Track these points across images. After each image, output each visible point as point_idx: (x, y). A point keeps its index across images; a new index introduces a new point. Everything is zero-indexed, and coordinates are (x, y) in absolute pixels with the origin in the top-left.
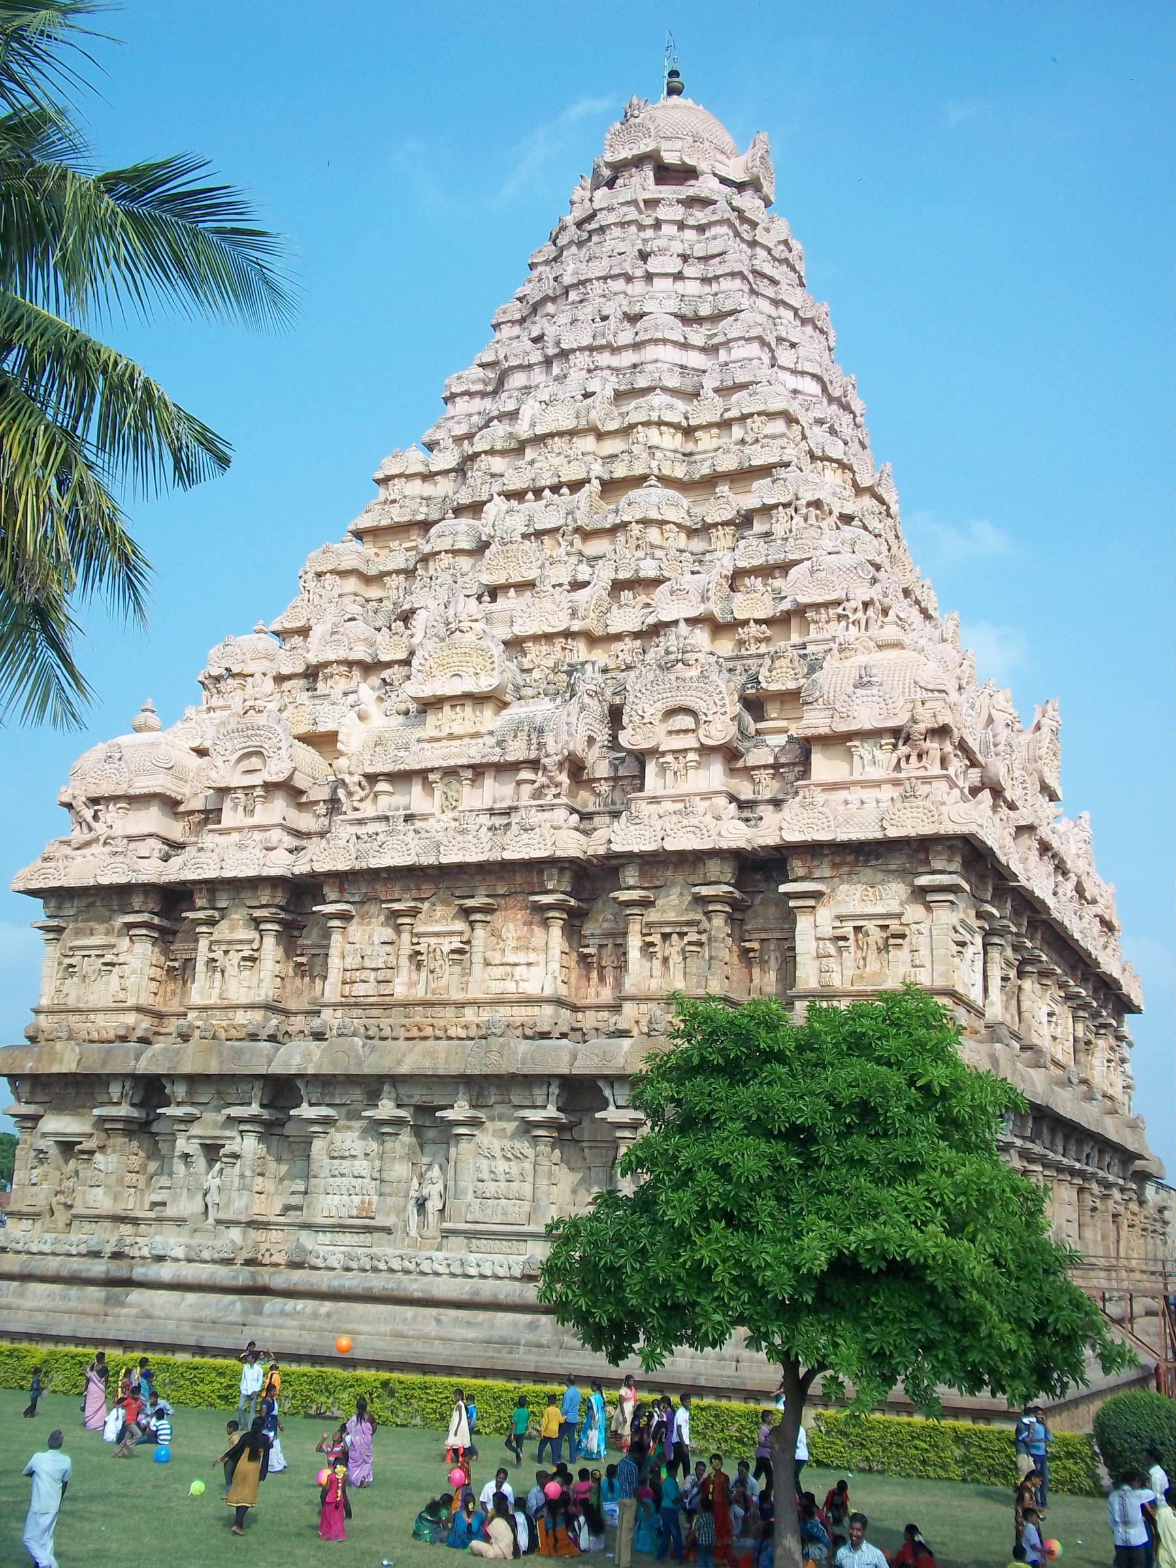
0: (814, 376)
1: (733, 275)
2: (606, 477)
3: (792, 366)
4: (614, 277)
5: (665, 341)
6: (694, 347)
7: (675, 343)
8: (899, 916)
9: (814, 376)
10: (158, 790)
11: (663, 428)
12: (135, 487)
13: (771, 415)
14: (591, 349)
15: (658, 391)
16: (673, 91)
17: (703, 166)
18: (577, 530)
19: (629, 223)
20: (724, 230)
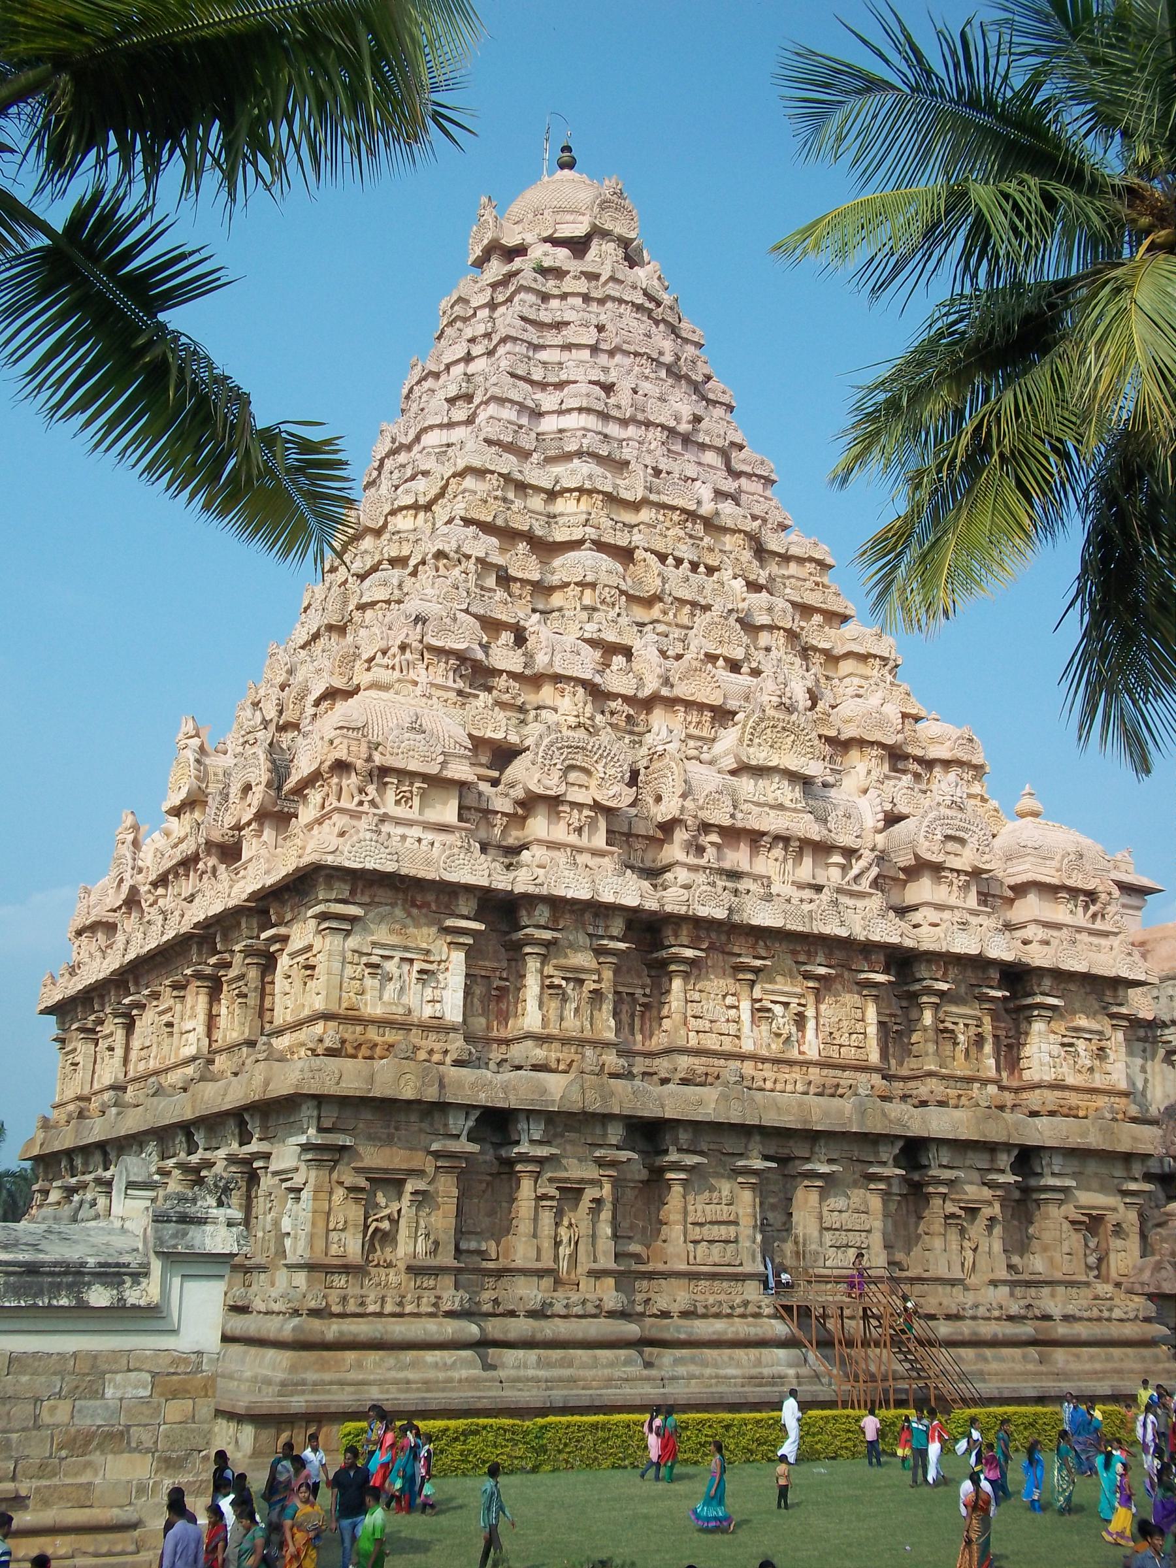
0: (580, 410)
1: (504, 340)
2: (362, 571)
3: (556, 407)
4: (424, 379)
5: (431, 427)
6: (459, 424)
7: (441, 426)
8: (309, 948)
9: (580, 410)
10: (98, 919)
11: (404, 512)
12: (876, 573)
13: (461, 474)
14: (393, 452)
15: (420, 476)
16: (562, 166)
17: (530, 238)
18: (330, 628)
19: (454, 321)
20: (522, 295)
